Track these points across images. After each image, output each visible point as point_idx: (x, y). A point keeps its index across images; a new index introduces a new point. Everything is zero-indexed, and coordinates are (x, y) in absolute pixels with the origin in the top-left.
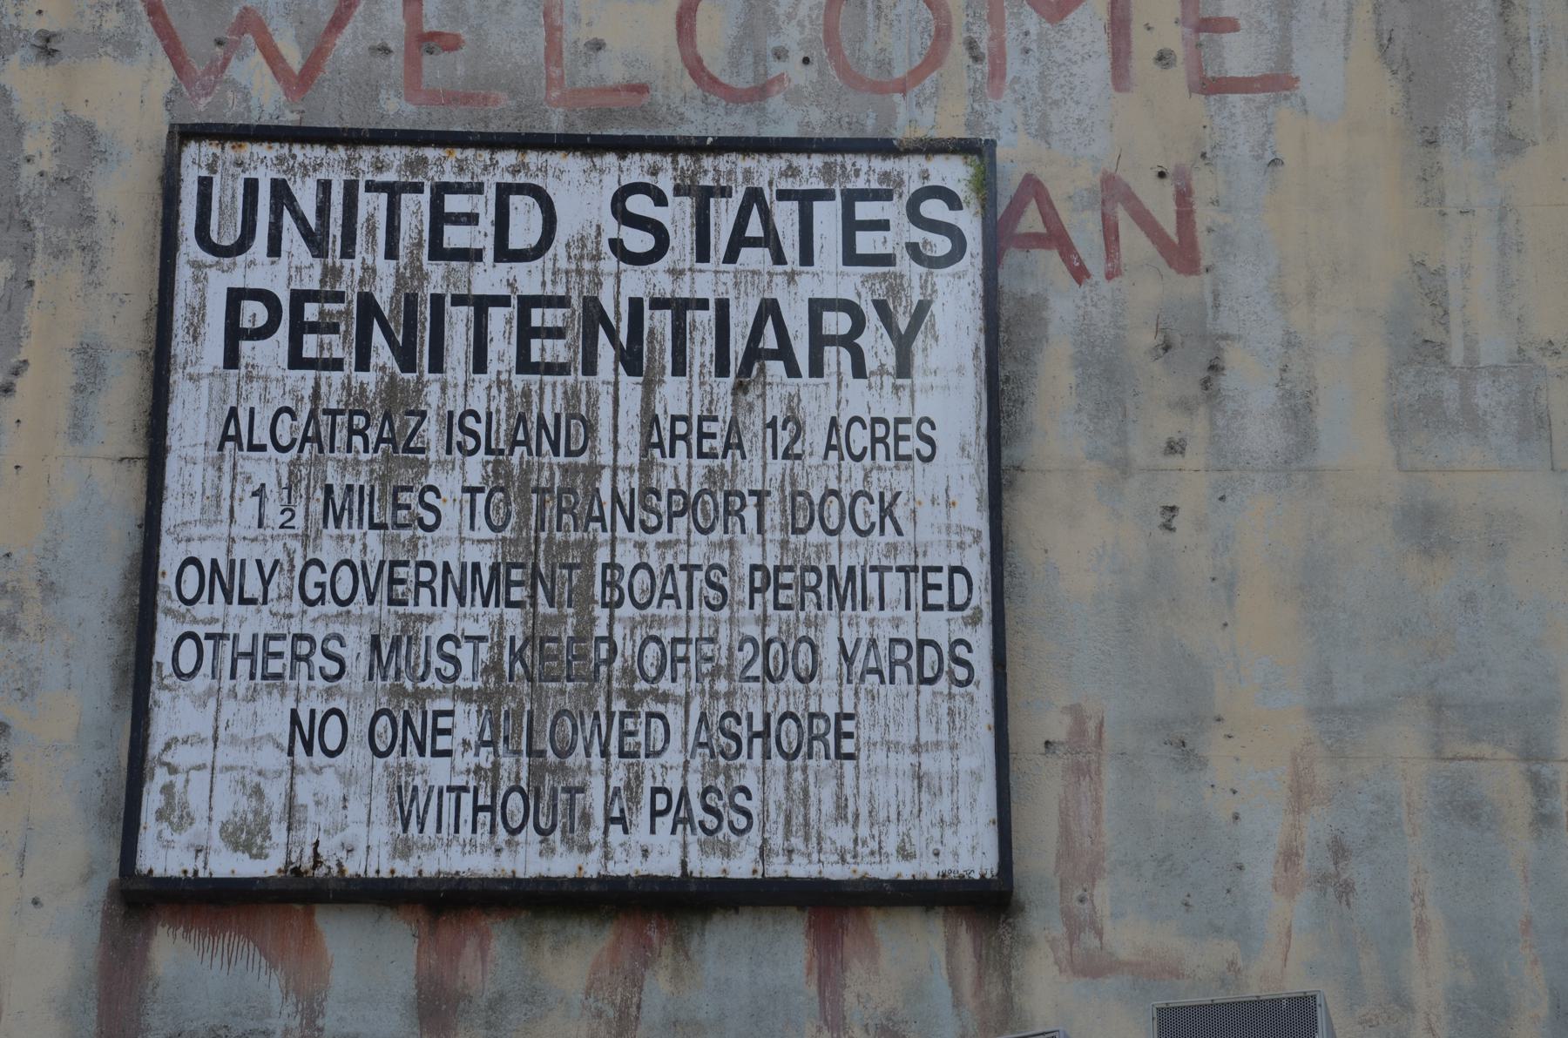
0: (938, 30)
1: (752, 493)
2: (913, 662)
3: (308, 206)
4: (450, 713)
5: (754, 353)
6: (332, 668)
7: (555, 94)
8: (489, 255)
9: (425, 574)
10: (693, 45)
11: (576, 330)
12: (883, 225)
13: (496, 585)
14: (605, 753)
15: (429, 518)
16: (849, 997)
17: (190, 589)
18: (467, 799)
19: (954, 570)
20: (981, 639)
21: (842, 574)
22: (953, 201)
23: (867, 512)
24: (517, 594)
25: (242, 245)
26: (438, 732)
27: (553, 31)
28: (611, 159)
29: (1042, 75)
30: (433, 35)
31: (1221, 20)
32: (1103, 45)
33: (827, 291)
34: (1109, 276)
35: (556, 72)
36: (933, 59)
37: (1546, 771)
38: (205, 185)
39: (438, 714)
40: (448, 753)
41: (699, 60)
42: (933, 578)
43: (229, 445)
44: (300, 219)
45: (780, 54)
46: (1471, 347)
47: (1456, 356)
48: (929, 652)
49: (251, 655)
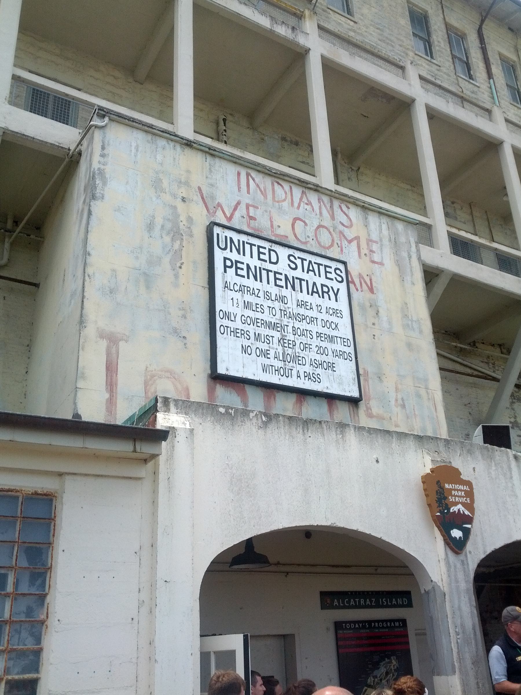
2: (343, 355)
5: (313, 292)
6: (248, 337)
7: (273, 234)
12: (330, 273)
14: (296, 363)
15: (262, 311)
20: (353, 352)
22: (341, 272)
24: (278, 329)
25: (225, 249)
28: (287, 248)
30: (251, 217)
32: (357, 250)
36: (332, 245)
38: (218, 235)
39: (267, 350)
40: (269, 358)
42: (345, 340)
43: (226, 288)
45: (308, 237)
46: (412, 317)
47: (410, 318)
49: (234, 332)
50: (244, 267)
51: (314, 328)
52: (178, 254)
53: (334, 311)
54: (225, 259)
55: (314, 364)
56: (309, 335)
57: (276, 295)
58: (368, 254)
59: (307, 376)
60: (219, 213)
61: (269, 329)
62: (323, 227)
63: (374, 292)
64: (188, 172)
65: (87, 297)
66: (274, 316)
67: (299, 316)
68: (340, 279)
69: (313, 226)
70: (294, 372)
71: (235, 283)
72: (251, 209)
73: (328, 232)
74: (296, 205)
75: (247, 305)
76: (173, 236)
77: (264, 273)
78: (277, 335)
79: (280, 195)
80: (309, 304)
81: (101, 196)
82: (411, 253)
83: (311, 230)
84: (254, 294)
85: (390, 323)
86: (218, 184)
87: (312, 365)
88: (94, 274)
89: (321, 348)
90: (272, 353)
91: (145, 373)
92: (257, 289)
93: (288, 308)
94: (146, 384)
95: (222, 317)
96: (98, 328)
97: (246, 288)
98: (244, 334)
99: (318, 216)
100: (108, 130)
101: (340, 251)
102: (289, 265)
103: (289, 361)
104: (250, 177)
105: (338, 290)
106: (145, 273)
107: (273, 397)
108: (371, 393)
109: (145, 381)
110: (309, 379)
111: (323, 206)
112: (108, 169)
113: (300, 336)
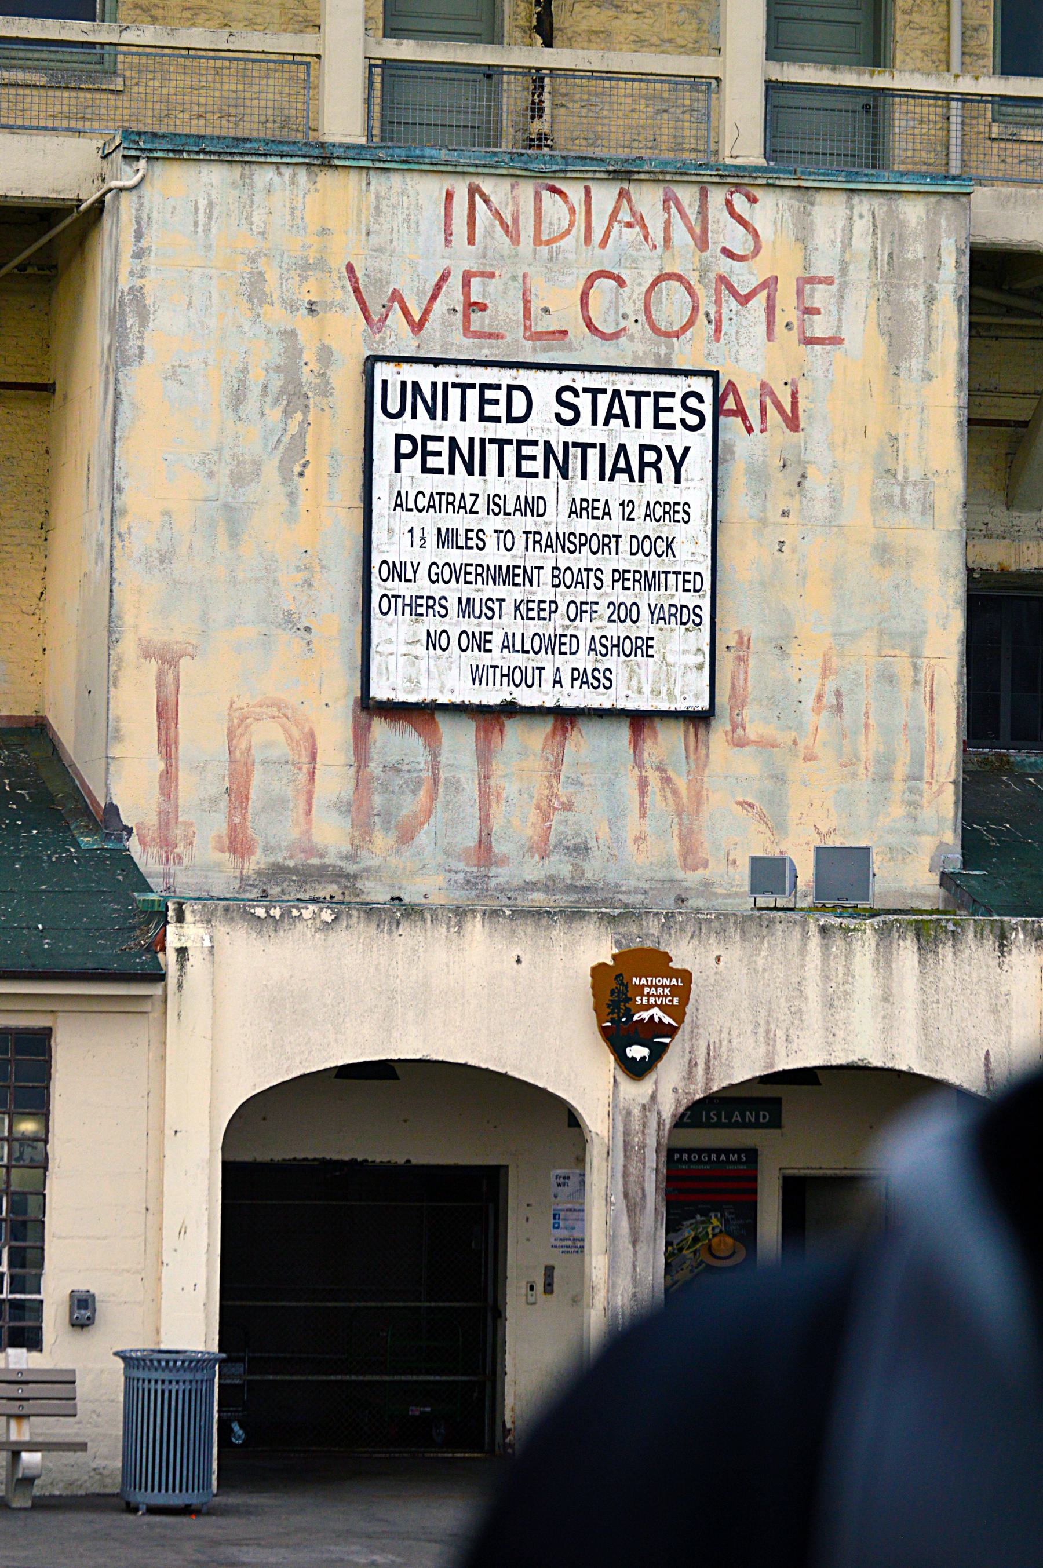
0: (693, 307)
1: (614, 536)
2: (678, 615)
3: (428, 395)
4: (491, 633)
5: (615, 470)
6: (443, 612)
7: (528, 334)
8: (504, 419)
9: (480, 570)
10: (588, 311)
11: (540, 458)
12: (670, 410)
13: (506, 575)
14: (553, 653)
15: (481, 545)
16: (646, 755)
17: (384, 576)
18: (498, 671)
19: (696, 573)
21: (650, 575)
22: (701, 400)
23: (661, 546)
25: (400, 414)
26: (486, 641)
27: (527, 302)
28: (555, 373)
29: (737, 332)
30: (476, 303)
31: (813, 308)
32: (763, 317)
33: (647, 442)
34: (762, 431)
35: (528, 323)
36: (691, 322)
37: (919, 662)
38: (385, 383)
39: (486, 633)
40: (490, 651)
41: (590, 319)
42: (687, 577)
44: (424, 401)
45: (625, 316)
47: (900, 477)
48: (685, 610)
50: (444, 447)
51: (608, 562)
52: (297, 446)
53: (667, 509)
54: (399, 438)
55: (599, 647)
56: (592, 580)
57: (518, 498)
58: (795, 323)
59: (580, 677)
60: (396, 316)
61: (495, 584)
62: (670, 276)
63: (798, 426)
64: (324, 231)
65: (118, 581)
66: (509, 550)
67: (572, 538)
68: (693, 420)
69: (640, 284)
70: (548, 675)
71: (420, 492)
72: (475, 282)
73: (683, 288)
74: (597, 236)
75: (446, 538)
76: (288, 405)
77: (492, 450)
78: (512, 594)
79: (555, 222)
80: (600, 505)
81: (137, 352)
82: (937, 286)
83: (635, 296)
84: (465, 508)
85: (834, 502)
86: (394, 243)
87: (594, 650)
88: (129, 529)
89: (623, 607)
90: (497, 639)
91: (229, 714)
92: (472, 495)
93: (546, 523)
94: (231, 735)
95: (384, 577)
96: (140, 639)
97: (444, 498)
98: (436, 605)
99: (659, 250)
100: (146, 190)
101: (712, 333)
102: (558, 416)
103: (536, 649)
104: (477, 197)
105: (687, 450)
106: (226, 506)
107: (497, 728)
108: (750, 689)
109: (229, 729)
110: (582, 683)
111: (677, 214)
112: (150, 284)
113: (568, 587)
